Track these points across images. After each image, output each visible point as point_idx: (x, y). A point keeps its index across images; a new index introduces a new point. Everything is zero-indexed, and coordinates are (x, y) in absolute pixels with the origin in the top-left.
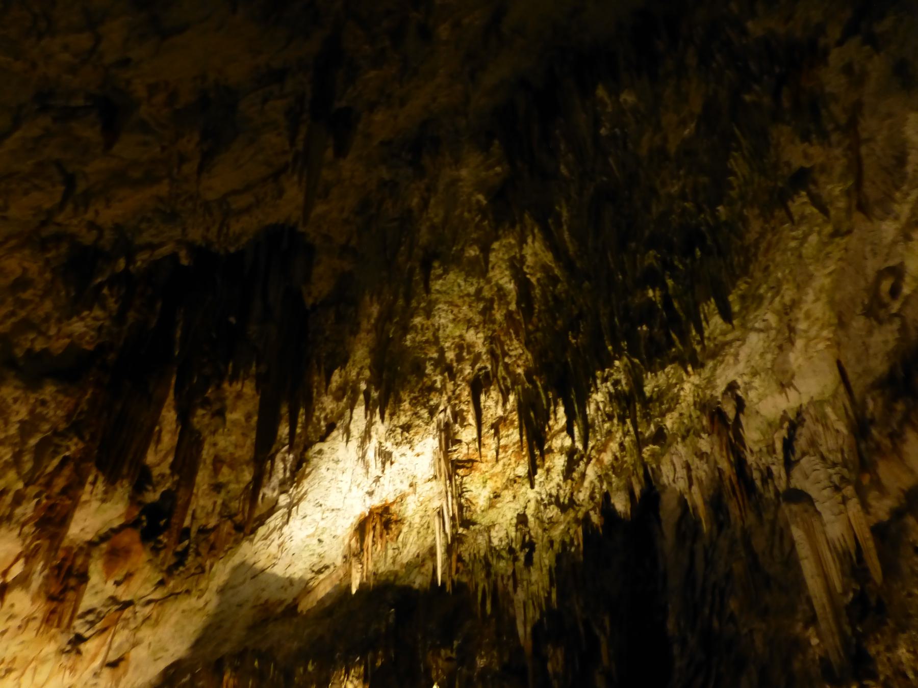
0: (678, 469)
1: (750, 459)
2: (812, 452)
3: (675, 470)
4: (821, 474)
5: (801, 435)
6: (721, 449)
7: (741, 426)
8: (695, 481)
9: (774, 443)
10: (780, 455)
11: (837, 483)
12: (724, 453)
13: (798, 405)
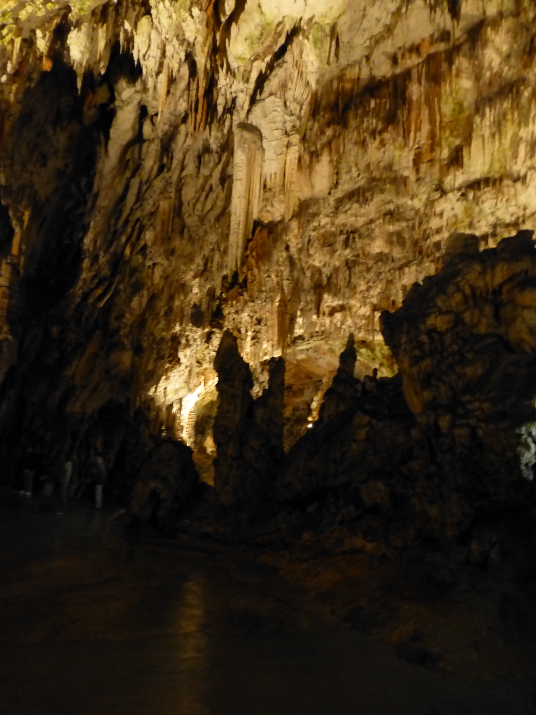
0: (152, 47)
1: (223, 80)
2: (278, 95)
3: (149, 46)
4: (279, 115)
5: (276, 75)
6: (204, 44)
7: (229, 37)
8: (165, 70)
9: (250, 72)
10: (252, 85)
11: (288, 130)
12: (206, 50)
13: (299, 17)
